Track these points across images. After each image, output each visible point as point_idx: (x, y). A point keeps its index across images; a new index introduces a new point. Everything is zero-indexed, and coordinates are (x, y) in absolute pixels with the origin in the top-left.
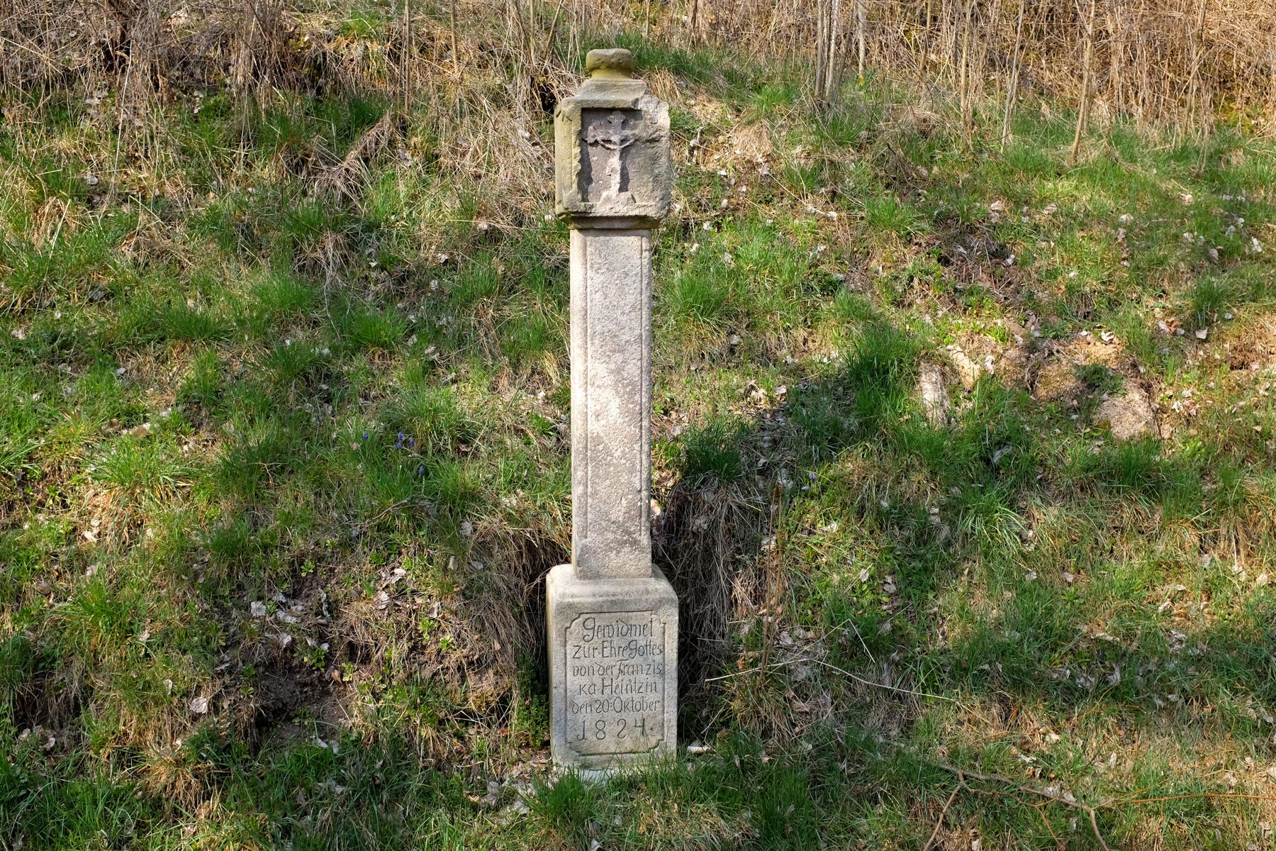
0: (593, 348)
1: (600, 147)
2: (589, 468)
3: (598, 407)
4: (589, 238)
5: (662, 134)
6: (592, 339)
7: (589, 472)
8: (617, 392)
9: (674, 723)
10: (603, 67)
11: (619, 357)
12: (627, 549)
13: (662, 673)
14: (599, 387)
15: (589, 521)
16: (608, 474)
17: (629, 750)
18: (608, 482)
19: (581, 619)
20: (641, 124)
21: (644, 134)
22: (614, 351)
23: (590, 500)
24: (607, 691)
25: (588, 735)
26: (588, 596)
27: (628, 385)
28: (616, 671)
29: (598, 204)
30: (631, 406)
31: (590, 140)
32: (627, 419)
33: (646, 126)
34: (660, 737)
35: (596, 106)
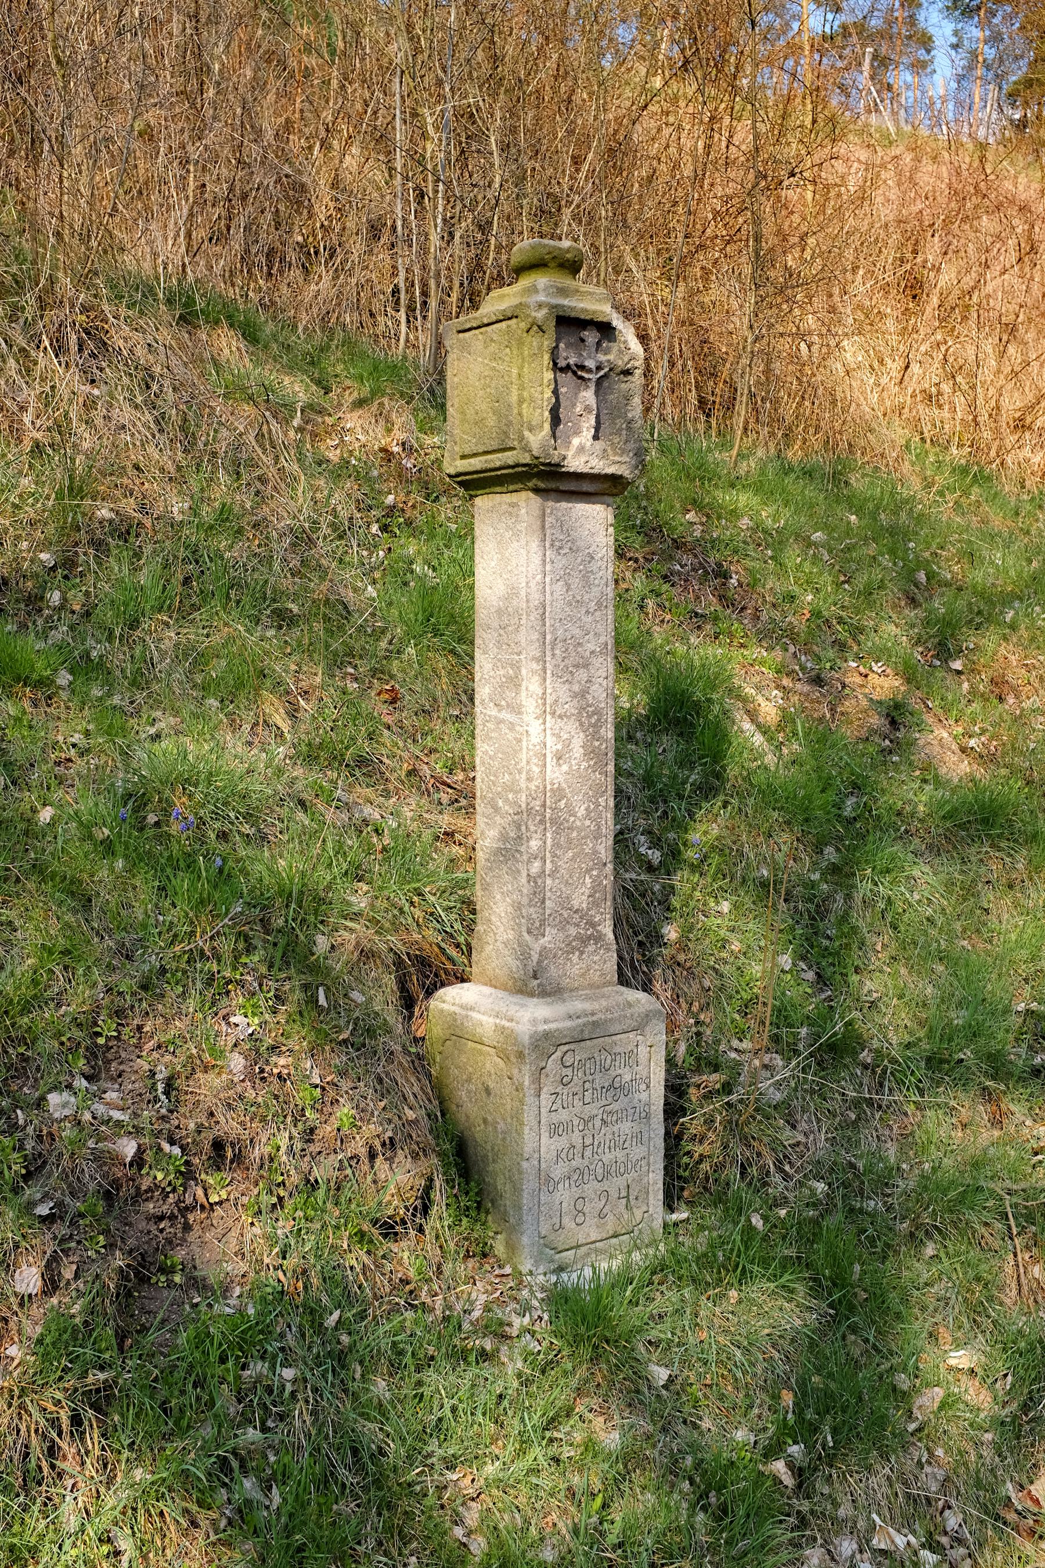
0: (554, 662)
1: (570, 374)
2: (548, 835)
3: (559, 747)
4: (550, 504)
5: (637, 364)
6: (553, 649)
7: (549, 842)
8: (581, 724)
9: (660, 1185)
10: (552, 264)
11: (582, 675)
12: (591, 948)
13: (648, 1117)
14: (560, 717)
15: (548, 912)
16: (570, 841)
17: (611, 1233)
18: (570, 854)
19: (559, 1054)
20: (615, 347)
21: (620, 363)
22: (577, 666)
23: (549, 881)
24: (588, 1153)
25: (566, 1221)
26: (563, 1019)
27: (594, 713)
28: (598, 1123)
29: (570, 454)
30: (597, 744)
31: (562, 363)
32: (592, 763)
33: (620, 351)
34: (645, 1209)
35: (573, 314)
